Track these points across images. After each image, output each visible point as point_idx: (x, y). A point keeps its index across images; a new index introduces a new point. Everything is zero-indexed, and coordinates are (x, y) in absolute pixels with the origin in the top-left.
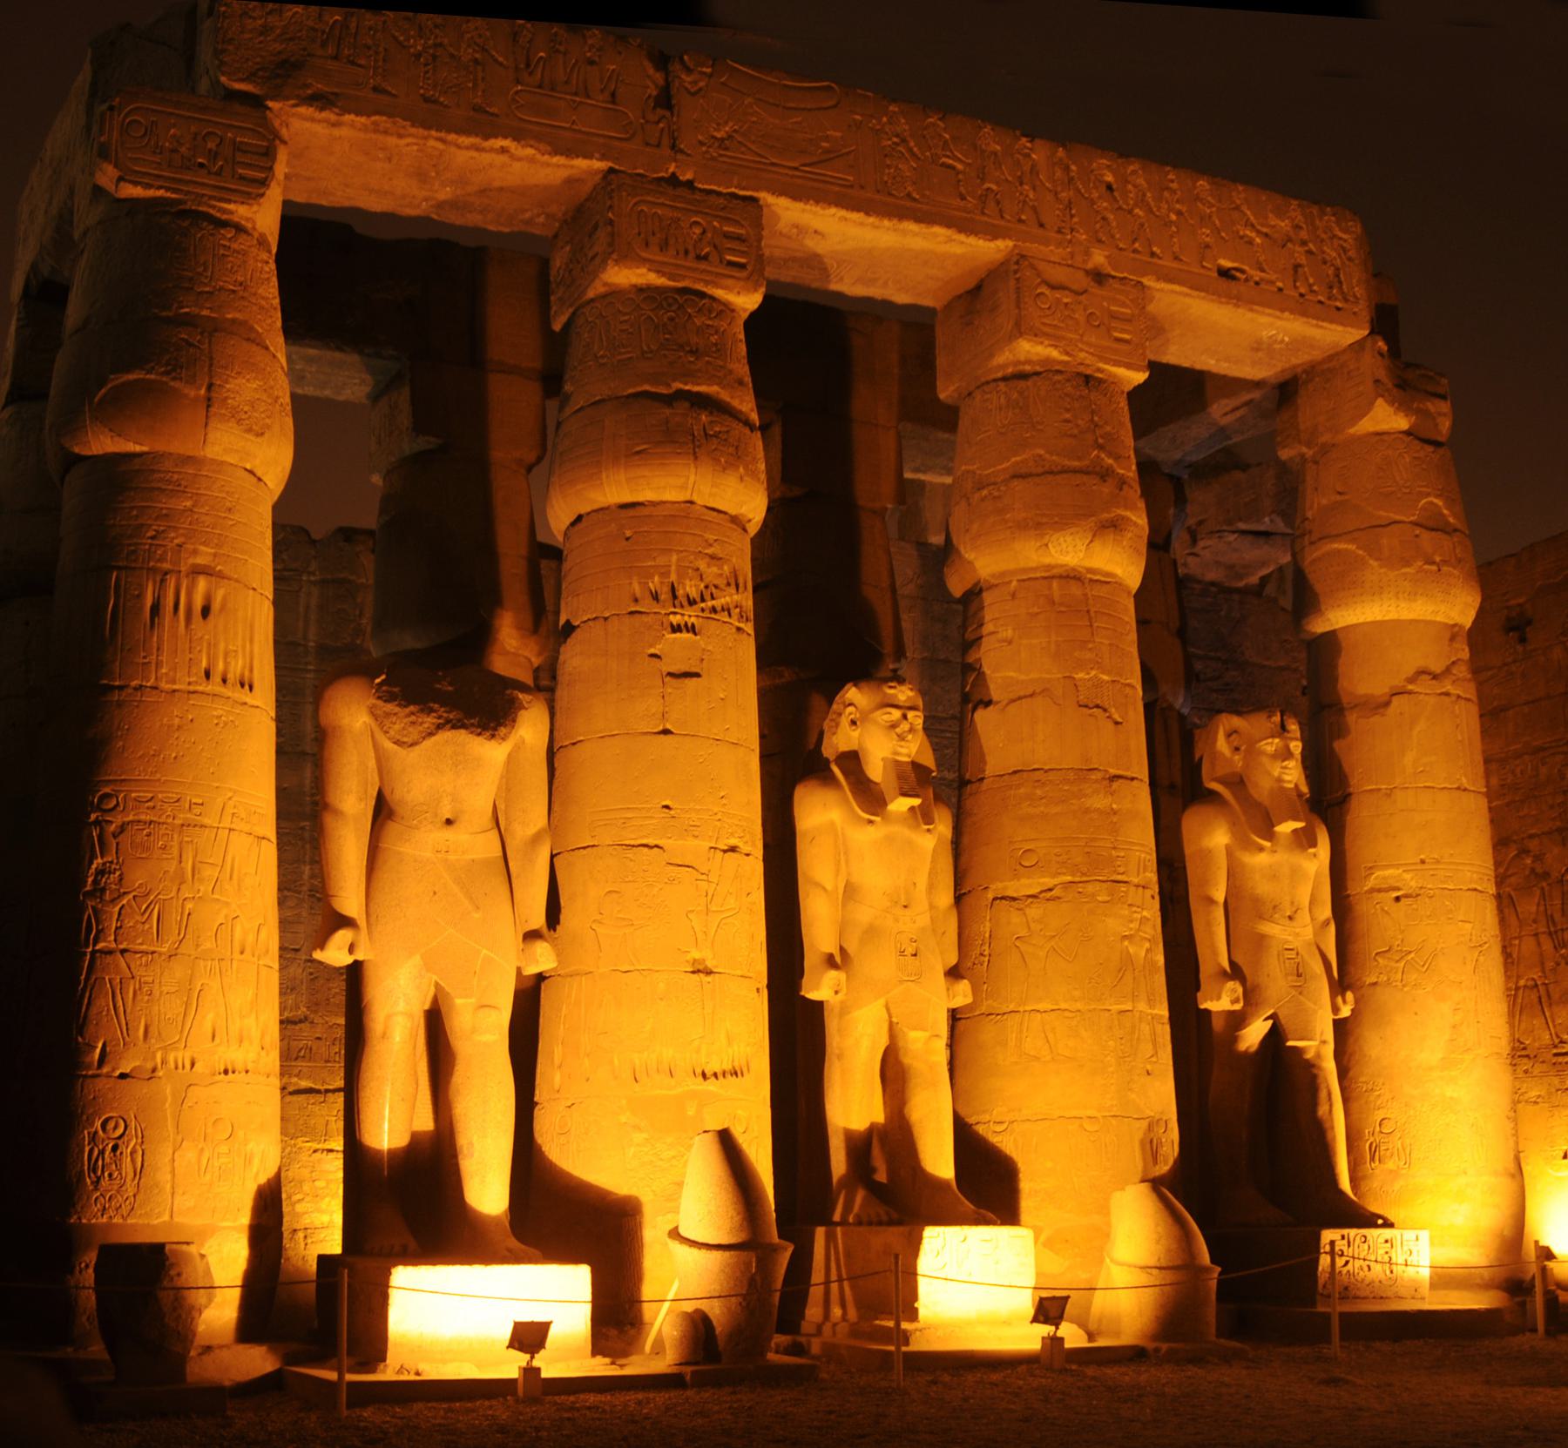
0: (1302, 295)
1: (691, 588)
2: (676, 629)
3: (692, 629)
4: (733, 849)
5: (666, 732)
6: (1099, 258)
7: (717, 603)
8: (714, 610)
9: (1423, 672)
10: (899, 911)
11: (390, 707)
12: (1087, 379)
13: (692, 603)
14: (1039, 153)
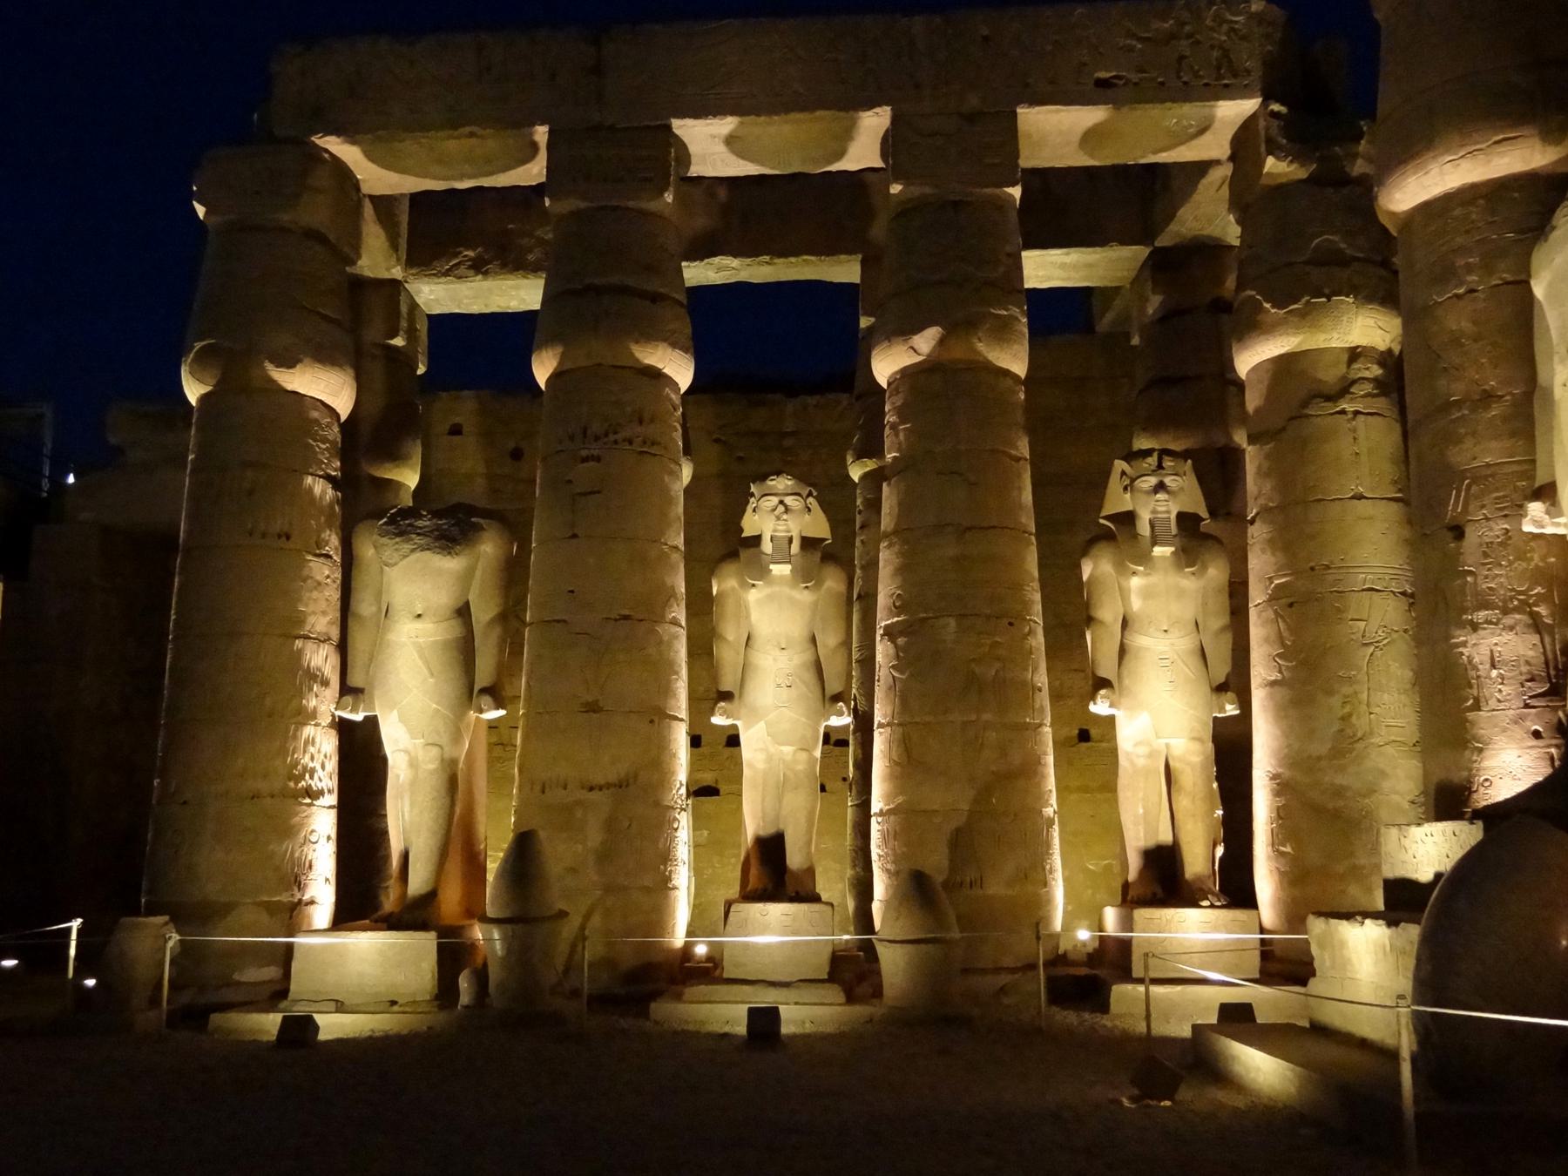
0: (1185, 83)
1: (596, 427)
2: (585, 460)
3: (598, 459)
4: (626, 618)
5: (575, 536)
6: (973, 101)
7: (619, 437)
8: (616, 442)
9: (1315, 396)
10: (778, 653)
11: (385, 540)
12: (956, 204)
13: (597, 438)
14: (918, 24)
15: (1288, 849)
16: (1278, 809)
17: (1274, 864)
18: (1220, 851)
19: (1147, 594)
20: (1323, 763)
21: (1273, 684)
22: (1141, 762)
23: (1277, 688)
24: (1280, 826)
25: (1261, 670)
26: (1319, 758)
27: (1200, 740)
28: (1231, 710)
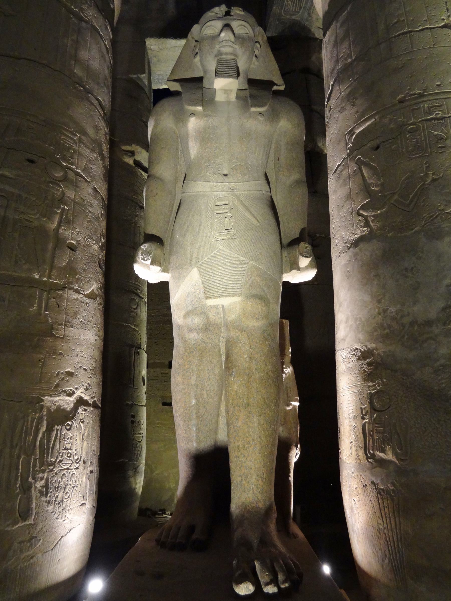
15: (389, 456)
16: (371, 397)
17: (368, 477)
18: (295, 456)
19: (205, 137)
20: (436, 330)
21: (356, 243)
22: (194, 336)
23: (361, 245)
24: (373, 421)
25: (342, 230)
26: (429, 323)
27: (261, 298)
28: (304, 273)
